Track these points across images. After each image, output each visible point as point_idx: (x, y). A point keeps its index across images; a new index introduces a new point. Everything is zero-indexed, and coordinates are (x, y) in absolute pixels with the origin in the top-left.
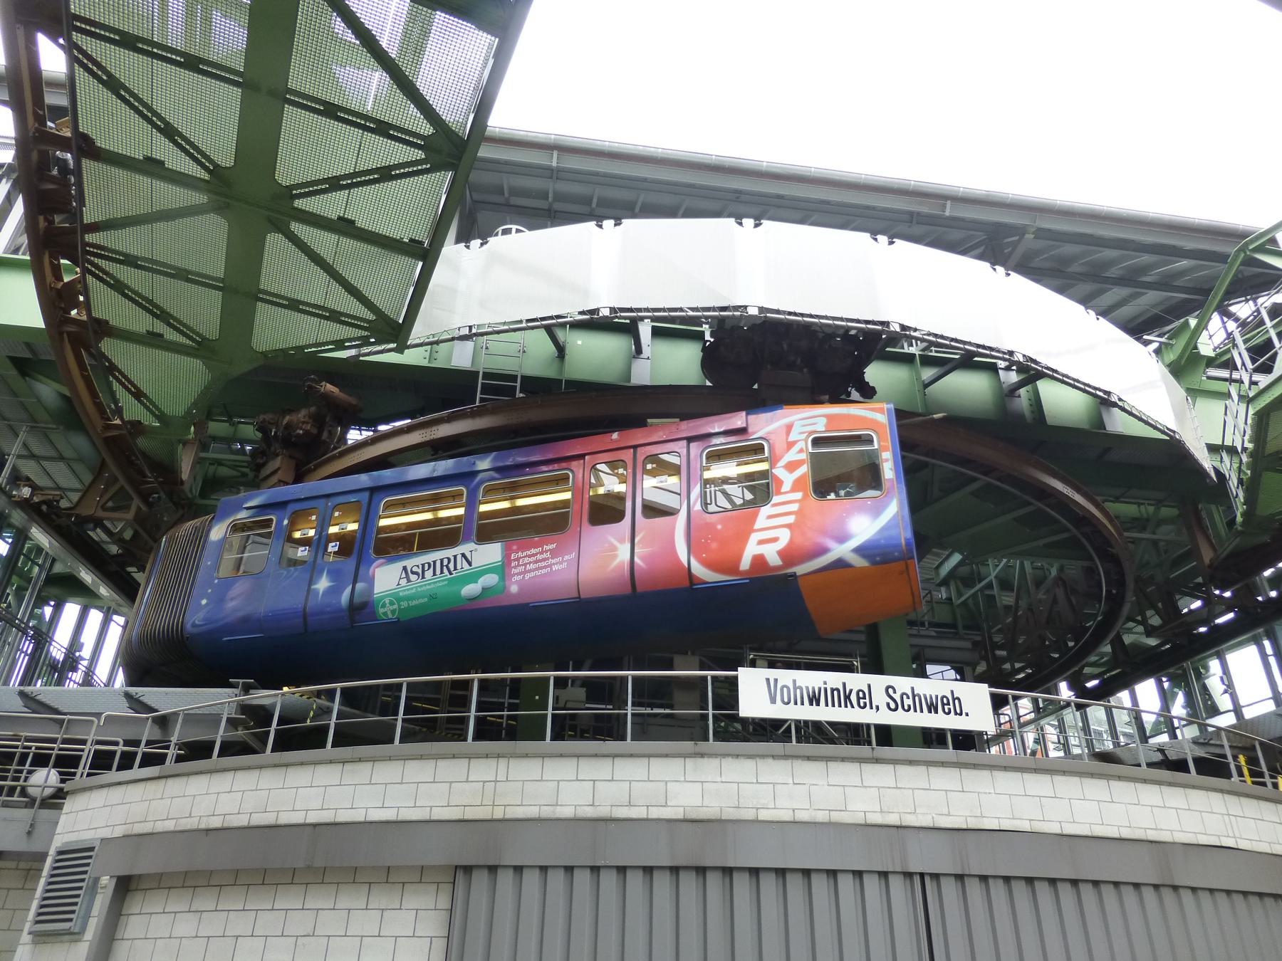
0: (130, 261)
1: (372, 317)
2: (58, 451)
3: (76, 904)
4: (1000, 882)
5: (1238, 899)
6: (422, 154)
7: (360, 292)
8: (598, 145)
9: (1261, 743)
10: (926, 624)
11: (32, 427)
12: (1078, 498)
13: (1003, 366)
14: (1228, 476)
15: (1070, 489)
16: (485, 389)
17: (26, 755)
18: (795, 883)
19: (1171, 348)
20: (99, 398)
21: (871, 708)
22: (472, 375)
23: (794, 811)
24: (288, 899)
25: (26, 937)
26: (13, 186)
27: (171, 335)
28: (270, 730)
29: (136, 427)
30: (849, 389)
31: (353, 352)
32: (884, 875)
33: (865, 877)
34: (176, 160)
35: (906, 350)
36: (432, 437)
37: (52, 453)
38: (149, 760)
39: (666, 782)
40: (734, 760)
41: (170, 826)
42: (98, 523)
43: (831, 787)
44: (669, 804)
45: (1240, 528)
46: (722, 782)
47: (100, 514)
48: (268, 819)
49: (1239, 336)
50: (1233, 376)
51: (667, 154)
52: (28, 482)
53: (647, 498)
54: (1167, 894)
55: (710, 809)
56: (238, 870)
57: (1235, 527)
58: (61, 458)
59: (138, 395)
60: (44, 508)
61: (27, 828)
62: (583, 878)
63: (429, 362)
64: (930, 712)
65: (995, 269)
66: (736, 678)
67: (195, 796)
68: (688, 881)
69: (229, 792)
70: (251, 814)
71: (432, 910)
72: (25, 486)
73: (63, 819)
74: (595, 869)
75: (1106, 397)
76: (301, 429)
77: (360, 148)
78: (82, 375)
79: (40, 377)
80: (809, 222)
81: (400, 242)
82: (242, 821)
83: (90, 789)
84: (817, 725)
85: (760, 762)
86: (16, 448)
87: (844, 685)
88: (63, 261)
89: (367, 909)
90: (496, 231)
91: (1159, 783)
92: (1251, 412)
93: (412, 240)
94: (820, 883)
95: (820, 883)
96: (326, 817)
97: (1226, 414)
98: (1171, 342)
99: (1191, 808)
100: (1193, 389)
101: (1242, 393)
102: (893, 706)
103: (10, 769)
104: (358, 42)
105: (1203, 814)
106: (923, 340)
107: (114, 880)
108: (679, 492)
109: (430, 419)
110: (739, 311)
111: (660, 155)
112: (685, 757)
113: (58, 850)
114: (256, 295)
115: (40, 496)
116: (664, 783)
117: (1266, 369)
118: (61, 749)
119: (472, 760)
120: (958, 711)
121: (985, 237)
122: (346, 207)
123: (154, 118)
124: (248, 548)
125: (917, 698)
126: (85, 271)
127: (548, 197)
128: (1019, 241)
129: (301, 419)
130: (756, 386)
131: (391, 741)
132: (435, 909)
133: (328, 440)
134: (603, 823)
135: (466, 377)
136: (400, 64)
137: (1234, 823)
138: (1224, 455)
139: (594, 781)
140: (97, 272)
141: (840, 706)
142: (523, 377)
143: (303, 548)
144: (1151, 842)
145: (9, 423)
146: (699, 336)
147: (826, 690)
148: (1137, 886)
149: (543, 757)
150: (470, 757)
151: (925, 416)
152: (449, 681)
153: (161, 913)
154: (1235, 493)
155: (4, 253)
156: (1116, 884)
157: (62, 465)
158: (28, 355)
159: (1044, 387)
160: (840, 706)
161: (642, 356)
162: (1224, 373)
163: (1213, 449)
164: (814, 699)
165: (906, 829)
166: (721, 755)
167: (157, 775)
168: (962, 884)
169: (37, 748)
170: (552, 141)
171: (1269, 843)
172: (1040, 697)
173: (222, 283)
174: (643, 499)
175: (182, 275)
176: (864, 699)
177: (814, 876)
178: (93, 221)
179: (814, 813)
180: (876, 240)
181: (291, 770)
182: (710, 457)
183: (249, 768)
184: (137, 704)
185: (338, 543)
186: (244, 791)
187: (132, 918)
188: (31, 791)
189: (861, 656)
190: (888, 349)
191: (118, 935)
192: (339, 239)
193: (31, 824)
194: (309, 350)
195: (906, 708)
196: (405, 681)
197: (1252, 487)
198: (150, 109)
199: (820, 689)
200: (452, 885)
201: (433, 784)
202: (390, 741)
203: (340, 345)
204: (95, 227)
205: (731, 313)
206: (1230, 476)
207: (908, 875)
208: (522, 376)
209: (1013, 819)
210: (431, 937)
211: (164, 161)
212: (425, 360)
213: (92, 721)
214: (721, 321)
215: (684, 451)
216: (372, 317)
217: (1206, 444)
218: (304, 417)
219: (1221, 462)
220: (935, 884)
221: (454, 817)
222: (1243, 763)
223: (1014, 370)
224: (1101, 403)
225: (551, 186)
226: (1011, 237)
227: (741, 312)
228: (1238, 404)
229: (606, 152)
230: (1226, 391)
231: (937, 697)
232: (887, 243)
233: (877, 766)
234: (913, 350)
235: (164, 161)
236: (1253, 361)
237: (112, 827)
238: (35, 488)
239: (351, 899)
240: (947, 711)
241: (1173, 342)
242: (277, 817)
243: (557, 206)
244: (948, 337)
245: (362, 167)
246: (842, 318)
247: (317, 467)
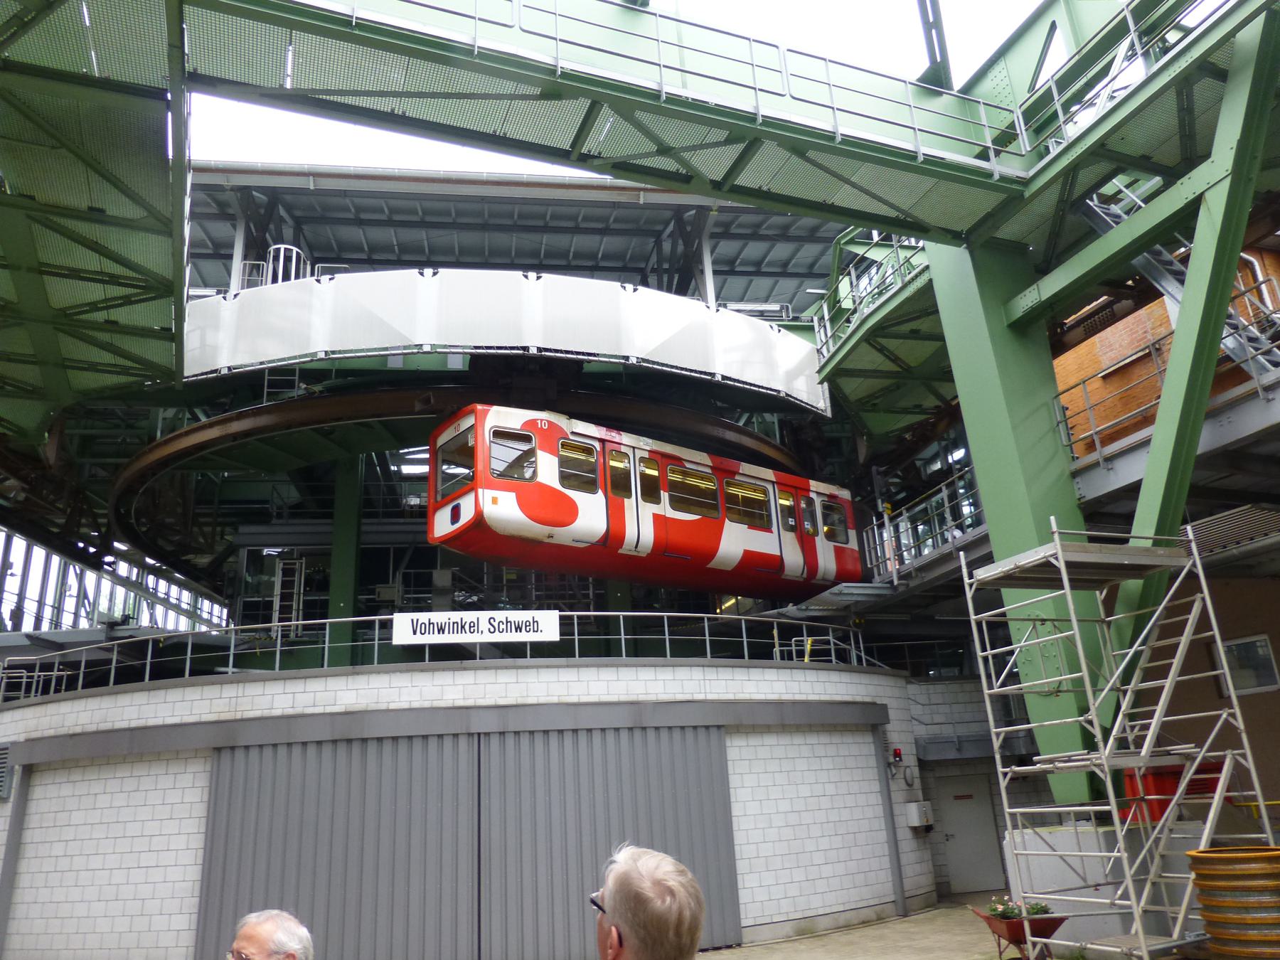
8: (345, 171)
41: (51, 733)
66: (391, 621)
82: (93, 728)
87: (462, 619)
96: (141, 723)
102: (492, 630)
107: (21, 768)
131: (183, 676)
176: (474, 627)
187: (36, 788)
191: (30, 798)
207: (470, 735)
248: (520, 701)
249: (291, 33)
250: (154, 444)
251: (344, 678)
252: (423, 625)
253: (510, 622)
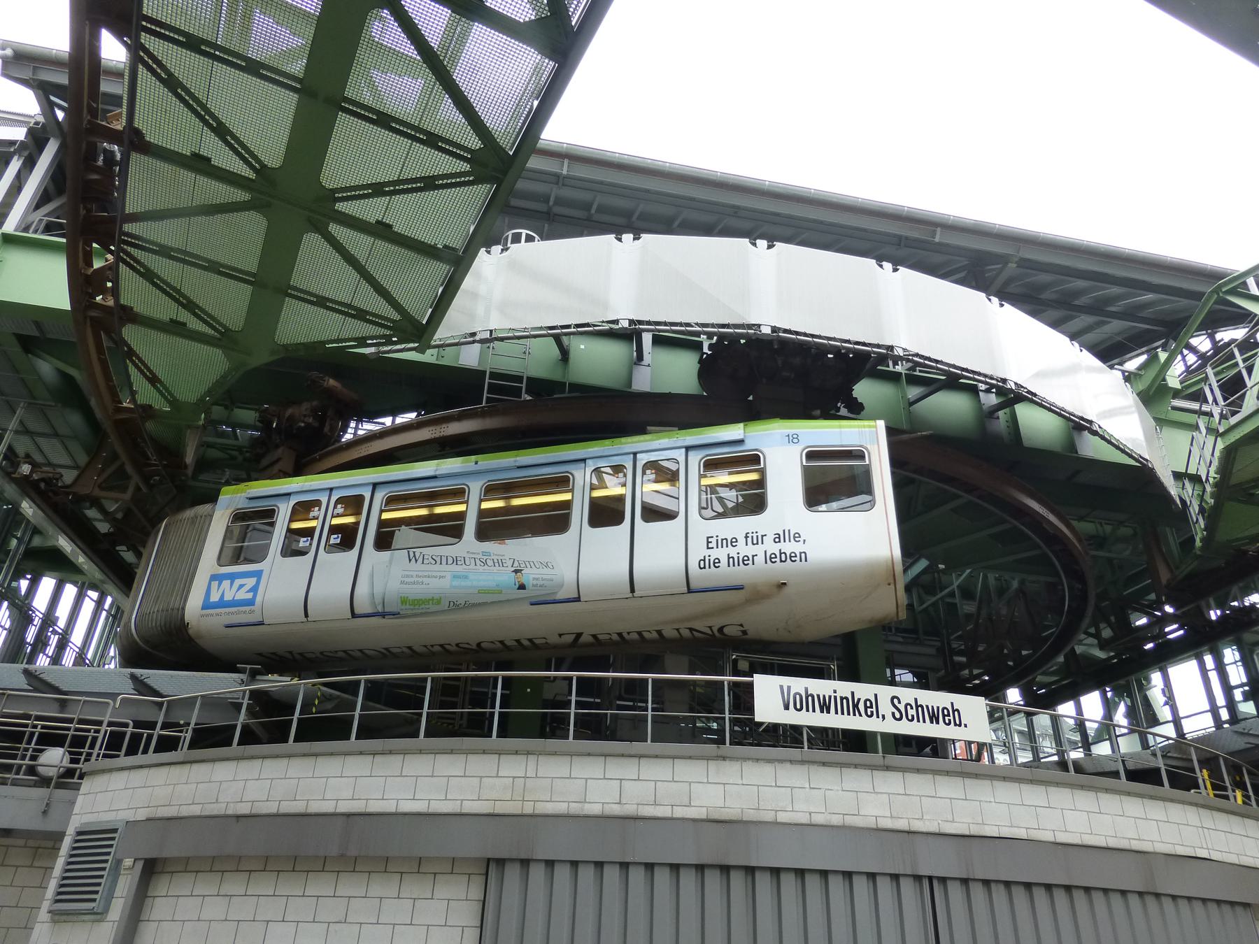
0: (164, 251)
1: (397, 317)
2: (53, 427)
3: (99, 884)
4: (1002, 887)
7: (389, 293)
8: (608, 157)
10: (893, 630)
11: (30, 403)
12: (1052, 518)
14: (1189, 503)
15: (1045, 510)
16: (492, 388)
17: (32, 734)
18: (813, 883)
19: (1140, 377)
20: (112, 381)
21: (878, 717)
22: (479, 374)
23: (810, 814)
24: (320, 885)
25: (43, 915)
26: (24, 164)
27: (195, 324)
29: (147, 411)
30: (839, 404)
31: (372, 350)
32: (895, 877)
33: (878, 878)
34: (223, 158)
35: (891, 368)
36: (442, 433)
37: (47, 430)
38: (167, 745)
39: (690, 783)
40: (754, 763)
41: (196, 810)
42: (96, 503)
44: (692, 804)
45: (1198, 553)
46: (743, 785)
47: (97, 492)
48: (297, 807)
51: (658, 165)
52: (28, 458)
53: (646, 501)
54: (1151, 901)
55: (730, 810)
57: (1194, 551)
58: (56, 435)
59: (153, 380)
60: (42, 485)
61: (43, 808)
62: (612, 874)
64: (932, 722)
65: (990, 300)
66: (750, 686)
67: (221, 782)
68: (713, 879)
69: (257, 780)
70: (280, 801)
72: (25, 463)
73: (80, 799)
74: (625, 866)
76: (303, 422)
77: (406, 157)
78: (99, 359)
79: (47, 357)
80: (797, 241)
81: (434, 247)
82: (271, 808)
83: (110, 770)
84: (824, 731)
86: (13, 424)
87: (853, 694)
88: (95, 245)
89: (398, 898)
90: (507, 234)
93: (445, 247)
94: (836, 884)
95: (836, 884)
97: (1192, 444)
98: (1140, 372)
100: (1160, 419)
102: (898, 715)
103: (20, 747)
104: (418, 58)
105: (1180, 826)
106: (908, 360)
107: (140, 865)
108: (677, 496)
110: (753, 329)
111: (667, 169)
113: (77, 831)
114: (285, 290)
115: (39, 473)
116: (688, 784)
117: (1237, 405)
118: (77, 730)
119: (501, 756)
120: (958, 723)
122: (386, 212)
123: (203, 113)
124: (249, 535)
125: (920, 709)
126: (118, 259)
128: (1001, 270)
129: (302, 413)
130: (751, 398)
131: (416, 735)
132: (467, 900)
133: (329, 434)
134: (632, 821)
135: (474, 376)
137: (1207, 834)
139: (621, 780)
140: (125, 257)
141: (849, 714)
143: (305, 539)
145: (8, 398)
146: (698, 346)
147: (835, 697)
148: (1123, 893)
149: (572, 756)
150: (499, 753)
151: (911, 433)
152: (463, 677)
155: (15, 230)
156: (1106, 891)
157: (55, 441)
158: (35, 333)
159: (1022, 410)
160: (849, 714)
161: (643, 363)
162: (1195, 406)
163: (1178, 476)
164: (825, 707)
165: (916, 835)
166: (742, 758)
167: (181, 760)
168: (966, 888)
169: (43, 727)
170: (564, 150)
171: (1238, 855)
173: (254, 277)
174: (642, 501)
175: (214, 267)
176: (871, 708)
177: (808, 877)
178: (131, 212)
179: (829, 817)
181: (320, 759)
182: (708, 465)
183: (277, 757)
184: (142, 687)
185: (340, 535)
187: (157, 900)
188: (40, 769)
189: (838, 659)
190: (879, 368)
192: (374, 242)
193: (47, 804)
194: (330, 345)
195: (910, 718)
196: (429, 676)
197: (1213, 516)
198: (204, 107)
199: (830, 697)
200: (484, 877)
202: (415, 735)
203: (362, 342)
204: (134, 218)
205: (745, 331)
206: (1191, 501)
207: (918, 878)
208: (527, 377)
209: (1011, 827)
211: (211, 158)
213: (108, 703)
214: (722, 337)
215: (682, 459)
216: (397, 317)
217: (1172, 471)
218: (306, 409)
219: (1183, 489)
220: (942, 887)
221: (485, 811)
222: (1206, 777)
223: (993, 392)
224: (1074, 428)
225: (555, 192)
228: (1206, 436)
231: (938, 708)
234: (899, 368)
236: (1225, 399)
237: (135, 810)
238: (35, 465)
239: (381, 887)
240: (947, 722)
241: (1142, 372)
243: (557, 210)
245: (406, 175)
247: (322, 457)
248: (975, 830)
249: (411, 144)
250: (337, 445)
251: (702, 764)
252: (798, 697)
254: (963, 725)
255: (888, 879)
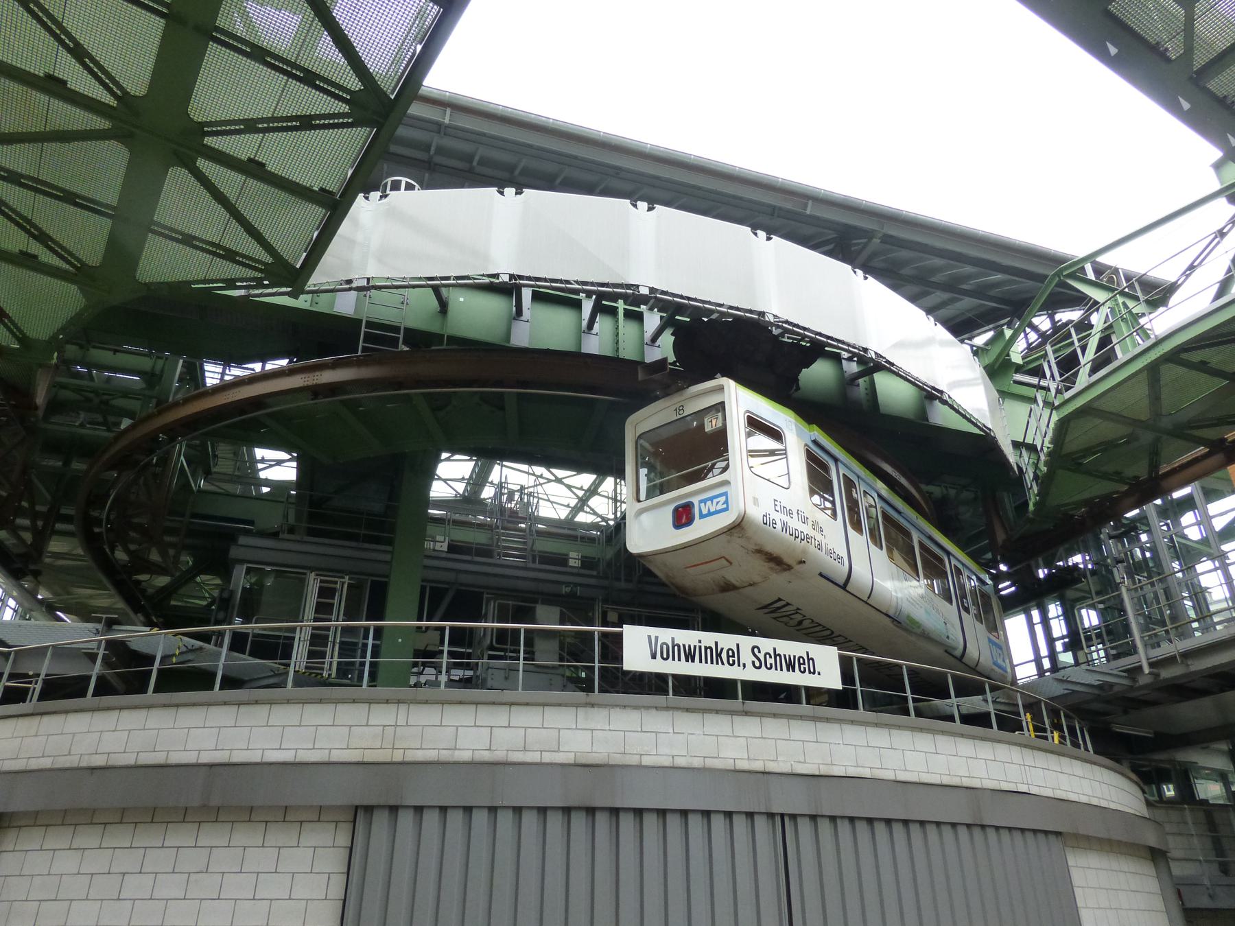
0: (14, 178)
1: (269, 260)
4: (846, 822)
5: (1029, 835)
6: (345, 108)
7: (261, 234)
8: (491, 108)
9: (1045, 703)
13: (845, 357)
14: (1024, 471)
18: (674, 822)
19: (986, 353)
21: (739, 665)
23: (673, 757)
24: (180, 836)
27: (46, 257)
28: (152, 669)
31: (242, 292)
32: (750, 815)
39: (559, 729)
41: (46, 763)
43: (706, 737)
44: (561, 749)
45: (1031, 516)
46: (610, 730)
48: (158, 758)
49: (1051, 353)
50: (1041, 383)
54: (977, 832)
55: (597, 755)
56: (155, 809)
57: (1027, 515)
62: (480, 818)
63: (311, 306)
64: (788, 670)
65: (855, 272)
66: (620, 635)
68: (578, 821)
70: (138, 753)
71: (330, 847)
74: (493, 810)
75: (939, 395)
77: (282, 94)
80: (676, 205)
81: (310, 190)
82: (129, 760)
85: (645, 713)
87: (716, 644)
89: (263, 846)
90: (384, 182)
91: (973, 737)
92: (1055, 418)
93: (322, 189)
94: (695, 822)
95: (695, 822)
97: (1030, 416)
98: (987, 347)
99: (997, 759)
101: (1050, 399)
102: (757, 664)
109: (314, 363)
111: (550, 125)
112: (577, 707)
117: (1072, 381)
119: (372, 705)
120: (812, 670)
121: (835, 236)
122: (258, 149)
123: (58, 32)
125: (778, 657)
127: (430, 150)
128: (865, 246)
132: (333, 847)
136: (341, 22)
137: (1028, 773)
138: (1024, 451)
139: (491, 727)
141: (712, 663)
142: (407, 330)
144: (967, 788)
147: (700, 647)
148: (954, 825)
149: (443, 704)
150: (370, 702)
153: (38, 850)
154: (1029, 486)
156: (938, 824)
159: (881, 379)
160: (712, 663)
161: (522, 318)
162: (1034, 381)
163: (1017, 445)
164: (690, 656)
166: (609, 705)
167: (31, 712)
172: (949, 672)
175: (70, 198)
176: (733, 657)
177: (669, 817)
180: (756, 234)
181: (182, 710)
186: (130, 731)
192: (245, 181)
194: (196, 286)
195: (769, 666)
198: (59, 25)
199: (695, 647)
200: (352, 823)
201: (332, 727)
203: (231, 283)
205: (624, 291)
206: (1026, 469)
207: (771, 816)
208: (405, 328)
209: (857, 766)
210: (329, 873)
212: (306, 303)
216: (269, 260)
217: (1012, 441)
219: (1020, 456)
220: (792, 823)
222: (1029, 720)
223: (854, 361)
225: (436, 141)
226: (860, 239)
227: (633, 290)
228: (1043, 409)
229: (499, 115)
230: (1033, 396)
231: (795, 657)
232: (765, 238)
233: (747, 719)
235: (67, 81)
236: (1061, 375)
239: (246, 836)
240: (802, 670)
242: (167, 756)
243: (438, 159)
244: (792, 323)
245: (279, 113)
246: (710, 301)
248: (824, 770)
249: (287, 81)
252: (665, 646)
253: (780, 655)
254: (816, 673)
255: (807, 819)
